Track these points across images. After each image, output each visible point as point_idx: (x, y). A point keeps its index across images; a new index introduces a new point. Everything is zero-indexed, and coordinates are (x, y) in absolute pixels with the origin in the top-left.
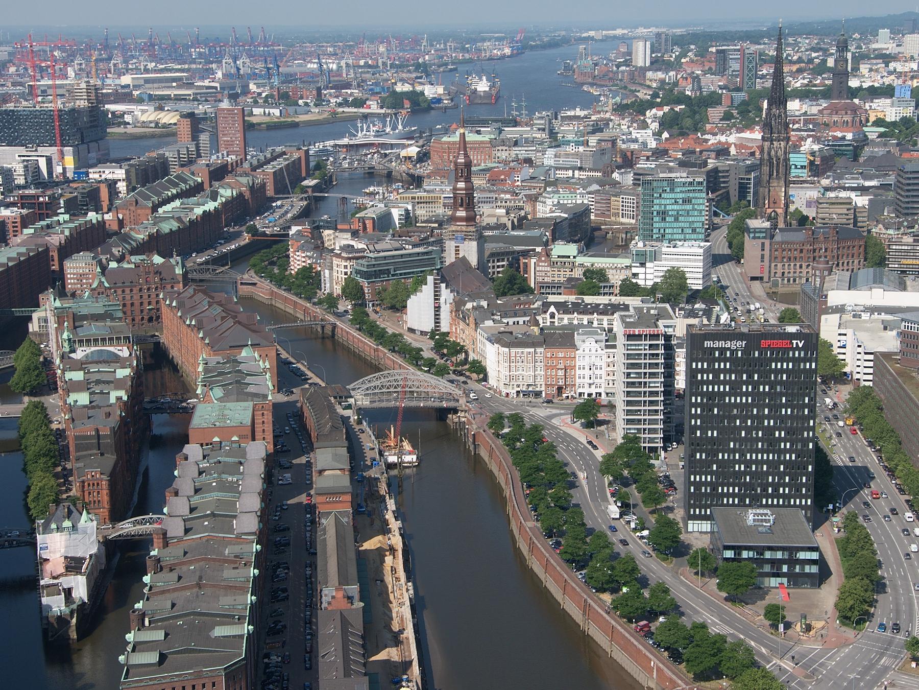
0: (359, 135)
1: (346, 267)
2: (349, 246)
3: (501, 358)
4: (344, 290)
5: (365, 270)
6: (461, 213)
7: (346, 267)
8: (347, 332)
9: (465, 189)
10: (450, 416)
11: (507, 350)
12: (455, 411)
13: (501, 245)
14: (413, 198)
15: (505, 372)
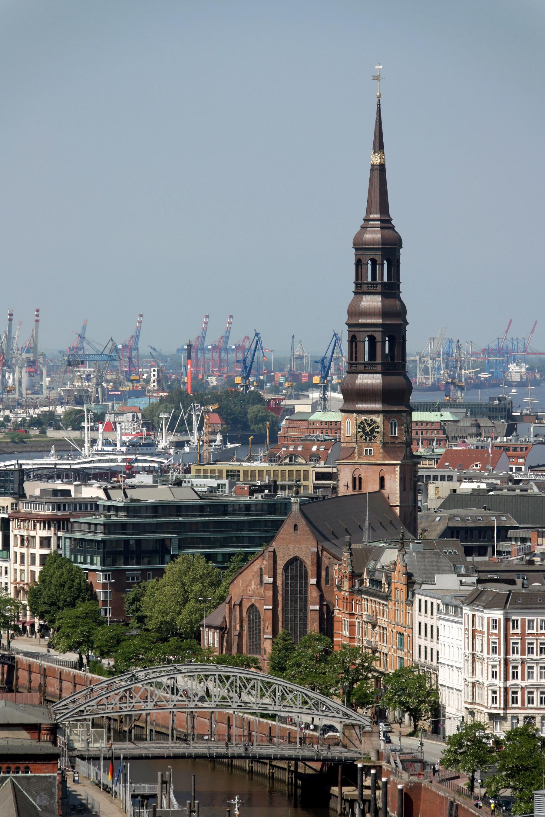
0: (86, 451)
1: (45, 542)
2: (55, 492)
3: (482, 642)
4: (35, 595)
5: (98, 537)
6: (372, 380)
7: (45, 542)
8: (44, 673)
9: (385, 313)
10: (335, 790)
11: (499, 615)
12: (348, 772)
13: (475, 511)
14: (232, 475)
15: (489, 681)
